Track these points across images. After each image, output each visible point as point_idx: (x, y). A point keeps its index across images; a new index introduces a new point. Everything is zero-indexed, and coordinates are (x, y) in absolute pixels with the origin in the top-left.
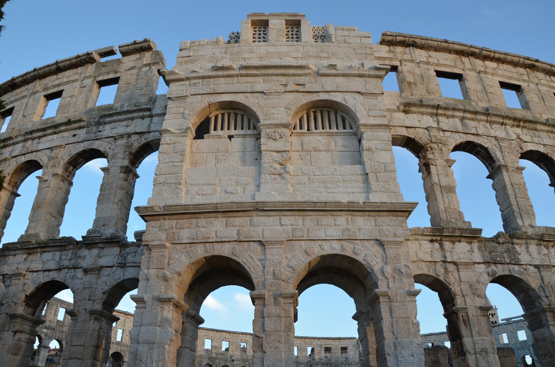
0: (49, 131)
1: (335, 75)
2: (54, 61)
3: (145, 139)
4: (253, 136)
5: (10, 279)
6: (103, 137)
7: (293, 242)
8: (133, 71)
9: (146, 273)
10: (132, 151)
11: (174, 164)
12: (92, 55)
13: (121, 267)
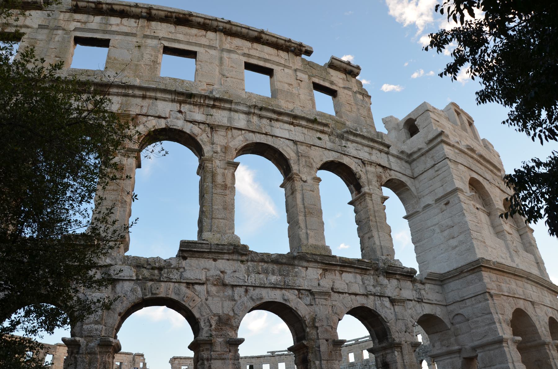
3: (390, 175)
6: (351, 155)
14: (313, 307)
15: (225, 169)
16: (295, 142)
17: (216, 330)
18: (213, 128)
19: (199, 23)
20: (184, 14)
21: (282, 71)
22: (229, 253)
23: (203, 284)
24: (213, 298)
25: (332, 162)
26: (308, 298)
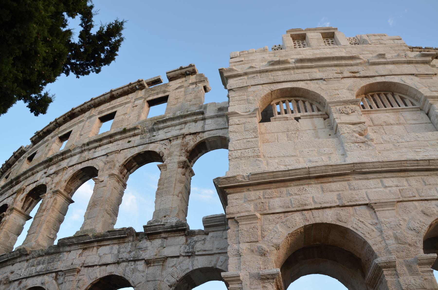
0: (105, 141)
1: (385, 64)
2: (108, 91)
3: (201, 138)
4: (320, 116)
5: (64, 276)
6: (158, 140)
7: (405, 203)
8: (181, 89)
9: (237, 248)
10: (189, 149)
11: (248, 140)
12: (142, 82)
13: (189, 256)
19: (79, 111)
20: (70, 112)
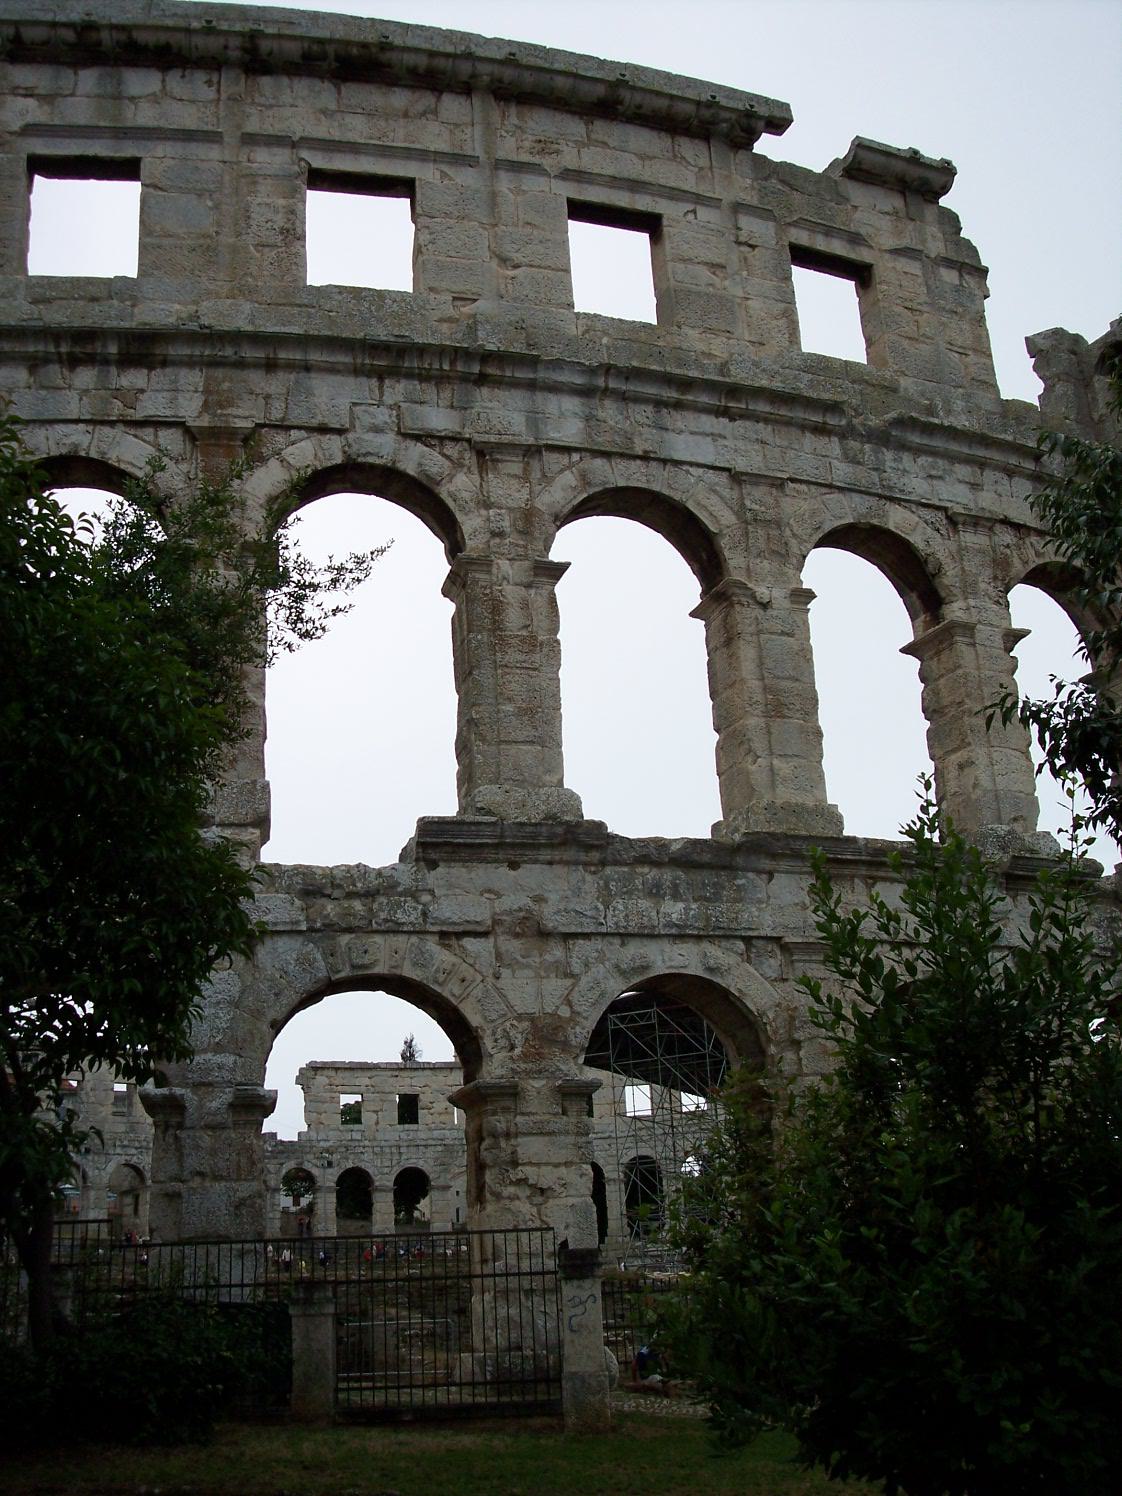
6: (913, 498)
14: (786, 984)
15: (528, 586)
16: (737, 477)
17: (525, 1057)
18: (485, 454)
19: (413, 71)
20: (365, 45)
21: (691, 217)
22: (552, 846)
23: (485, 934)
24: (514, 972)
25: (850, 528)
26: (772, 961)
